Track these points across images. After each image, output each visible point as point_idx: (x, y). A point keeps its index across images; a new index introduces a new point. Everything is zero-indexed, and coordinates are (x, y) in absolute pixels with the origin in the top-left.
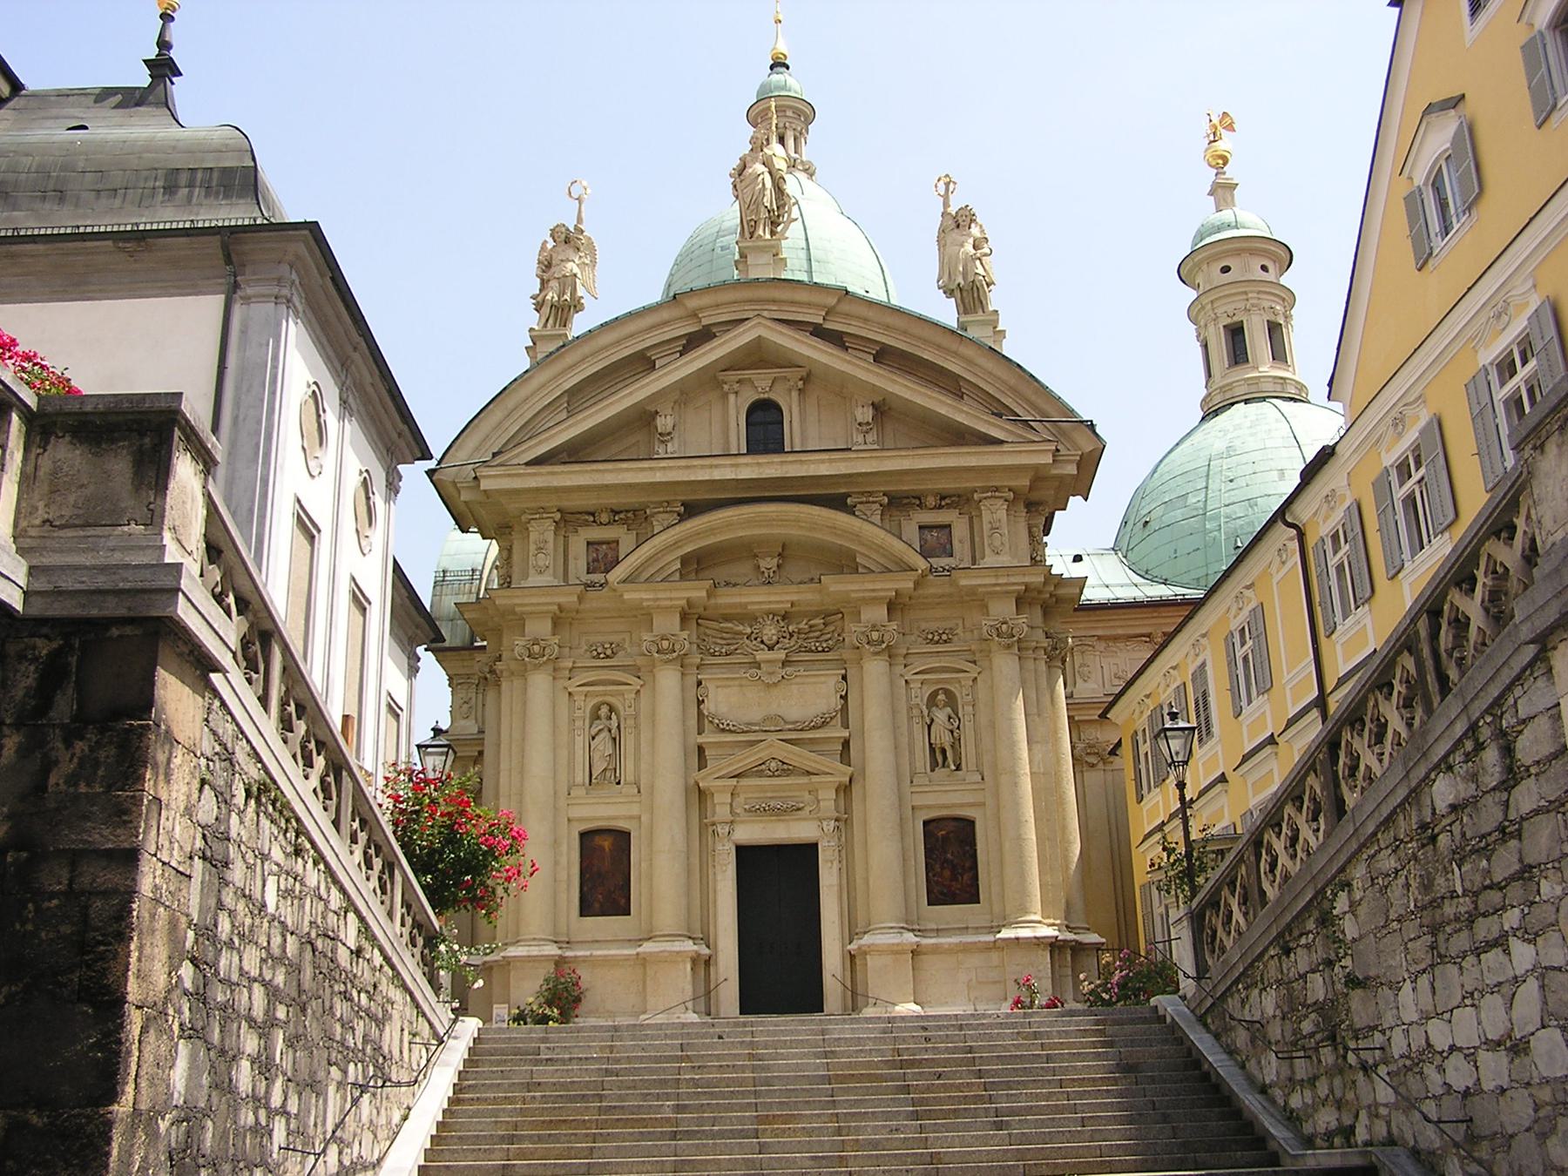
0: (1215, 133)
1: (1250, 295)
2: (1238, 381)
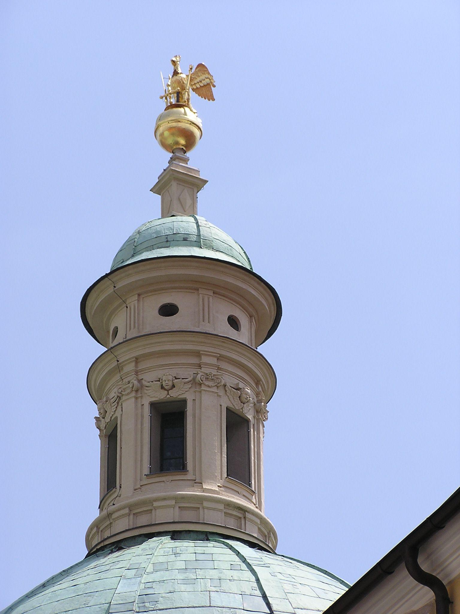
0: (179, 95)
1: (205, 359)
2: (164, 499)
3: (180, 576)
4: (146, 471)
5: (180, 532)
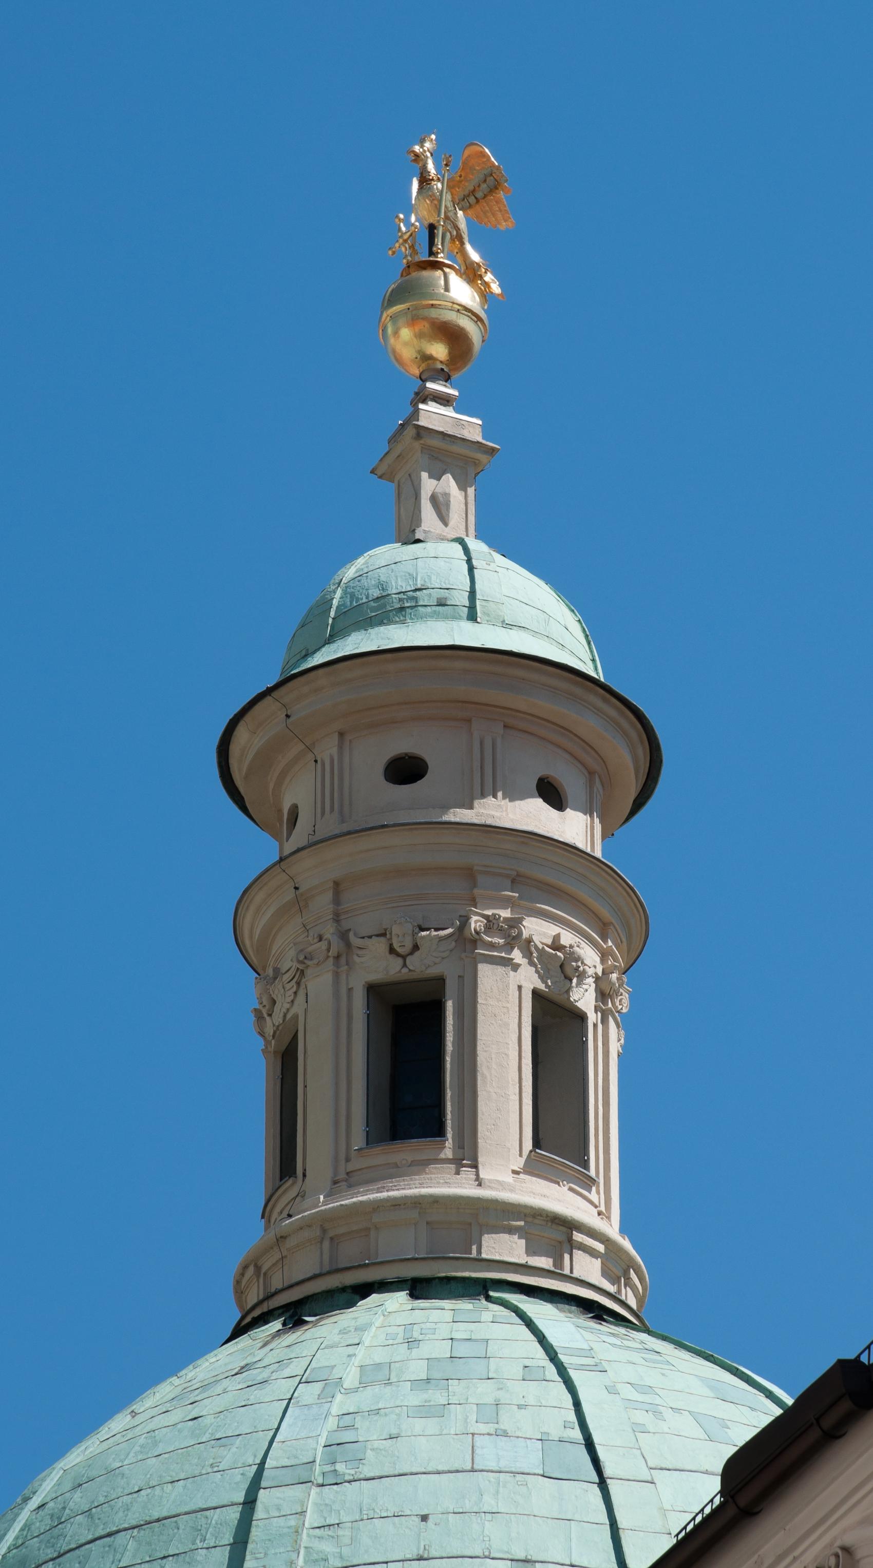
3: (415, 1399)
4: (358, 1140)
5: (428, 1281)
